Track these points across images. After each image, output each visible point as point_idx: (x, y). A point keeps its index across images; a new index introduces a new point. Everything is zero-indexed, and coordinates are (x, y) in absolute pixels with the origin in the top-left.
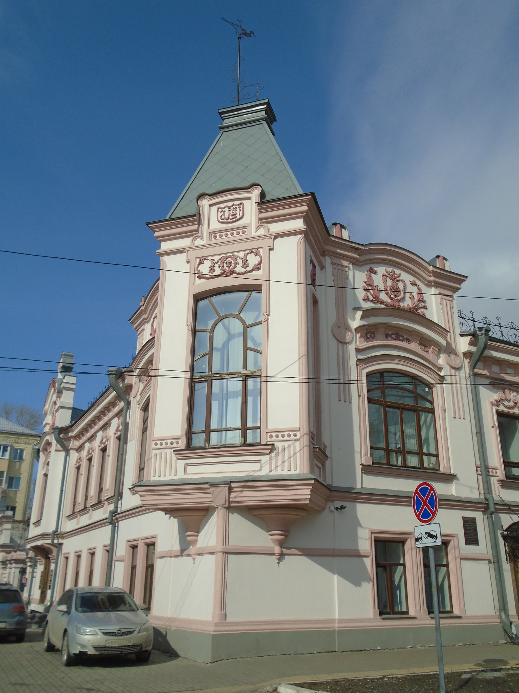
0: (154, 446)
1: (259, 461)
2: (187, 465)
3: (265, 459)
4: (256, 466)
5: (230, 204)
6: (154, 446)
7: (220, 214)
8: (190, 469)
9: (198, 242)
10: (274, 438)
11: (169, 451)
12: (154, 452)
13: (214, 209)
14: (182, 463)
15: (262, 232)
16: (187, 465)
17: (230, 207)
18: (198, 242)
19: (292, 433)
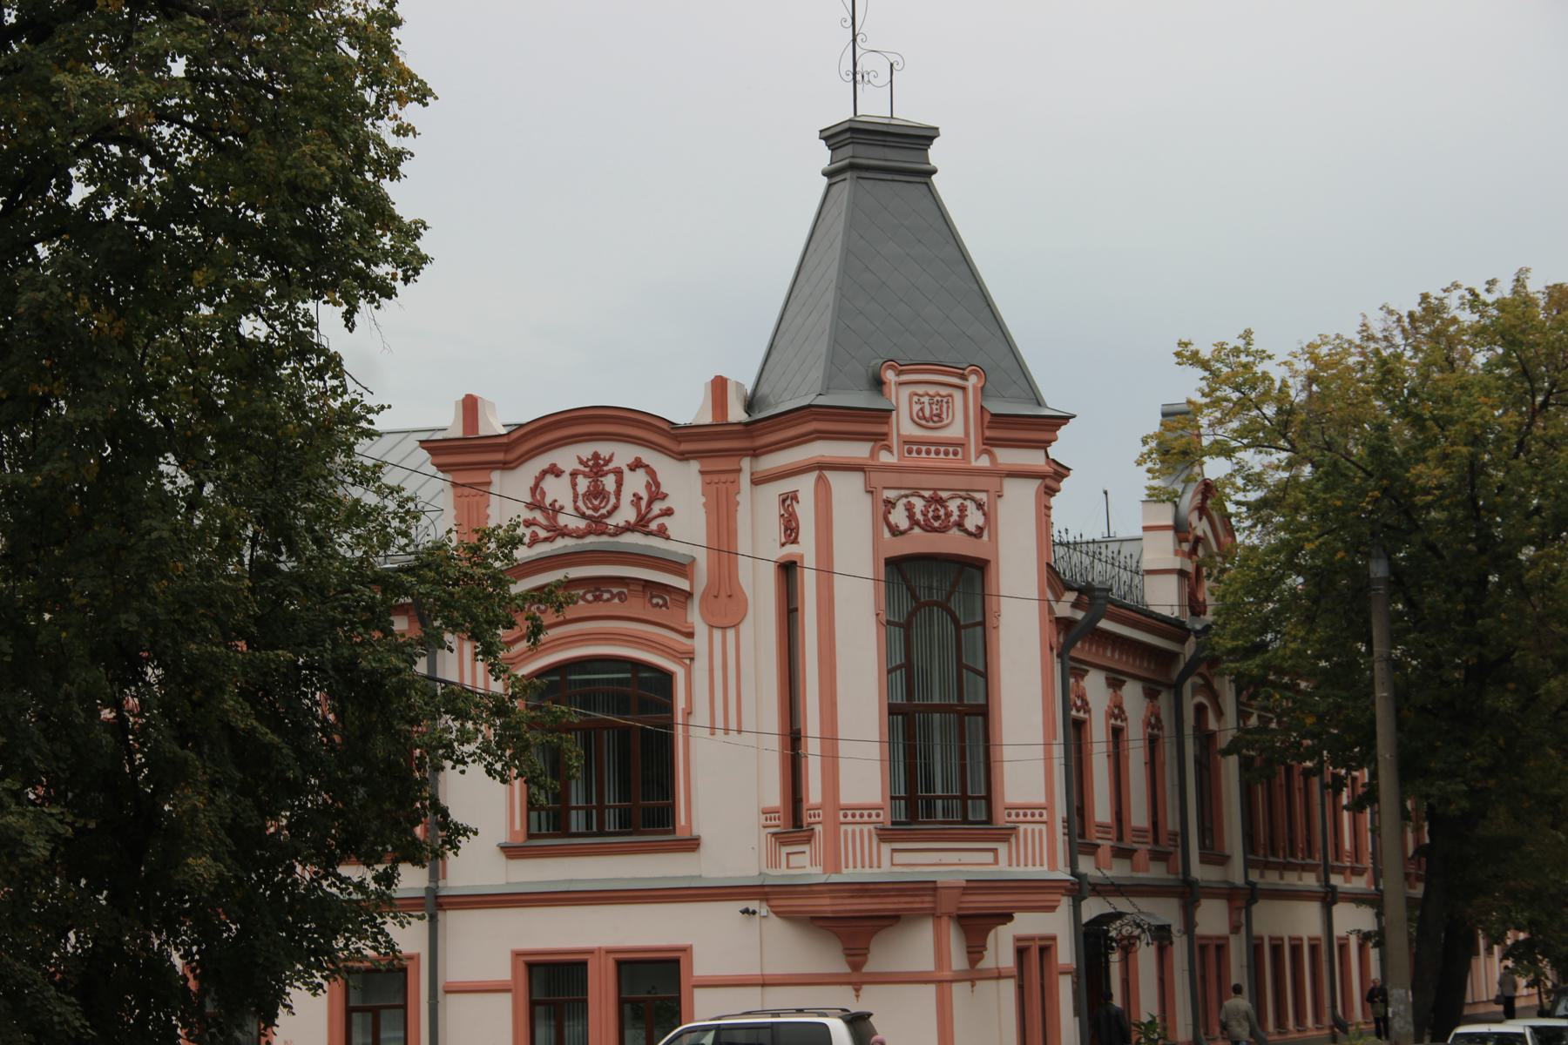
0: (842, 819)
1: (995, 850)
2: (894, 850)
3: (1002, 848)
4: (989, 857)
5: (932, 390)
6: (842, 819)
7: (916, 408)
8: (899, 858)
9: (885, 458)
10: (1021, 818)
11: (866, 828)
12: (843, 828)
13: (905, 392)
14: (886, 848)
15: (984, 462)
16: (894, 850)
17: (932, 397)
18: (885, 458)
19: (1037, 812)
